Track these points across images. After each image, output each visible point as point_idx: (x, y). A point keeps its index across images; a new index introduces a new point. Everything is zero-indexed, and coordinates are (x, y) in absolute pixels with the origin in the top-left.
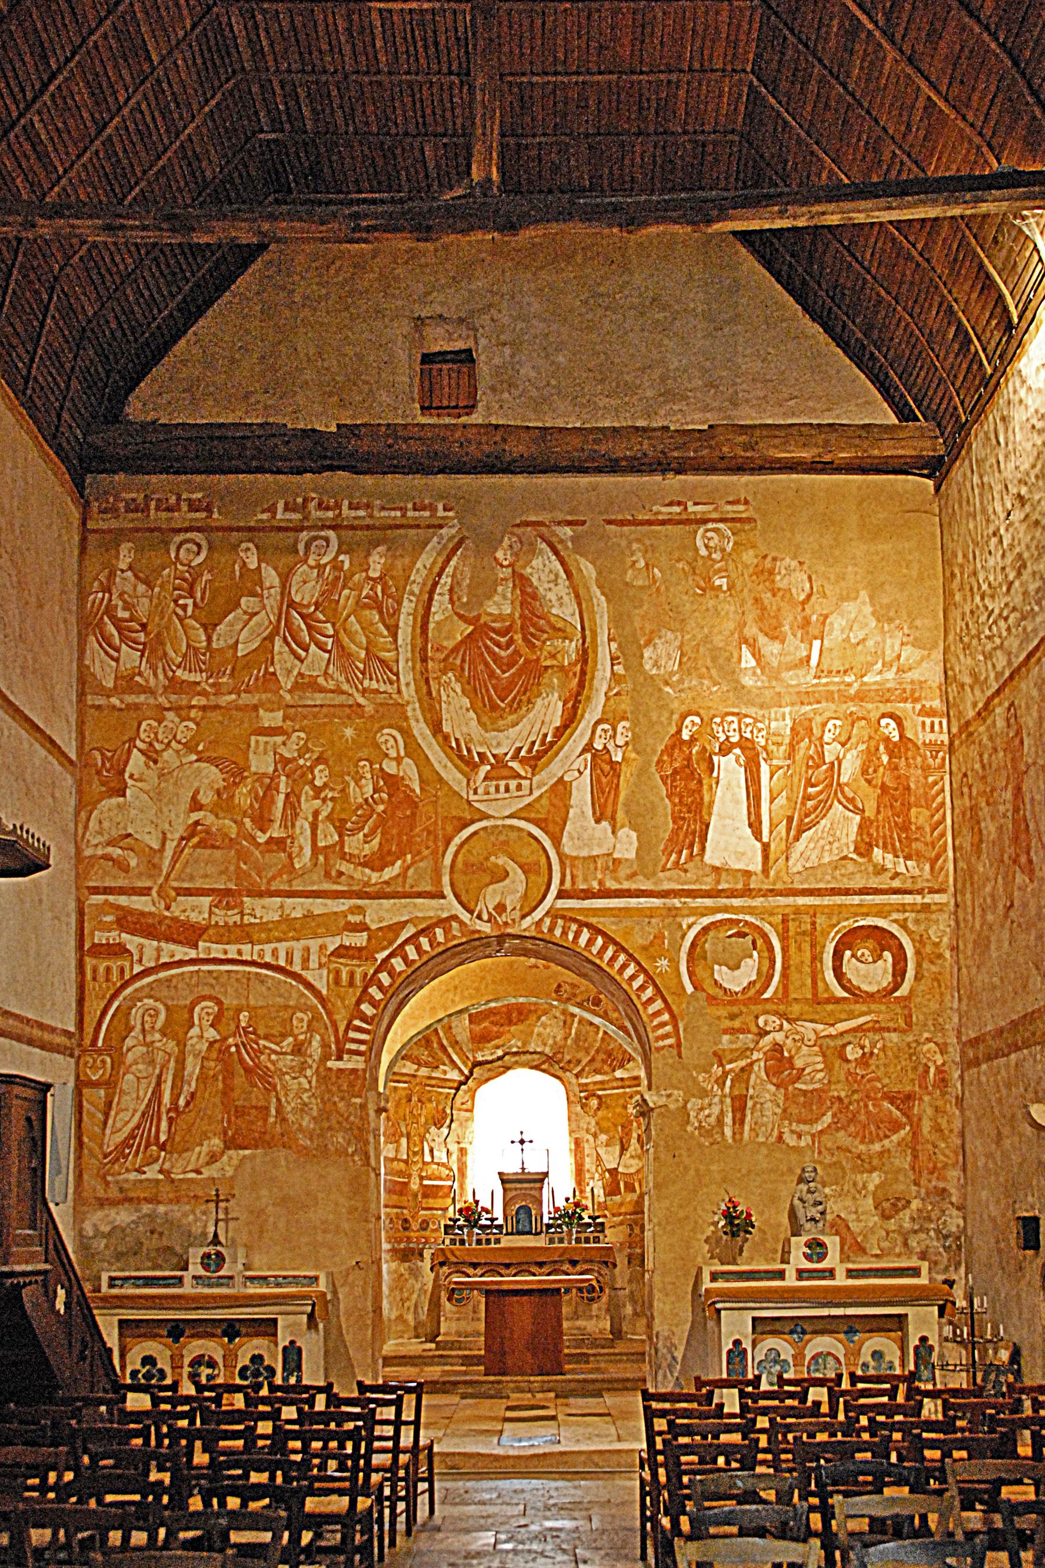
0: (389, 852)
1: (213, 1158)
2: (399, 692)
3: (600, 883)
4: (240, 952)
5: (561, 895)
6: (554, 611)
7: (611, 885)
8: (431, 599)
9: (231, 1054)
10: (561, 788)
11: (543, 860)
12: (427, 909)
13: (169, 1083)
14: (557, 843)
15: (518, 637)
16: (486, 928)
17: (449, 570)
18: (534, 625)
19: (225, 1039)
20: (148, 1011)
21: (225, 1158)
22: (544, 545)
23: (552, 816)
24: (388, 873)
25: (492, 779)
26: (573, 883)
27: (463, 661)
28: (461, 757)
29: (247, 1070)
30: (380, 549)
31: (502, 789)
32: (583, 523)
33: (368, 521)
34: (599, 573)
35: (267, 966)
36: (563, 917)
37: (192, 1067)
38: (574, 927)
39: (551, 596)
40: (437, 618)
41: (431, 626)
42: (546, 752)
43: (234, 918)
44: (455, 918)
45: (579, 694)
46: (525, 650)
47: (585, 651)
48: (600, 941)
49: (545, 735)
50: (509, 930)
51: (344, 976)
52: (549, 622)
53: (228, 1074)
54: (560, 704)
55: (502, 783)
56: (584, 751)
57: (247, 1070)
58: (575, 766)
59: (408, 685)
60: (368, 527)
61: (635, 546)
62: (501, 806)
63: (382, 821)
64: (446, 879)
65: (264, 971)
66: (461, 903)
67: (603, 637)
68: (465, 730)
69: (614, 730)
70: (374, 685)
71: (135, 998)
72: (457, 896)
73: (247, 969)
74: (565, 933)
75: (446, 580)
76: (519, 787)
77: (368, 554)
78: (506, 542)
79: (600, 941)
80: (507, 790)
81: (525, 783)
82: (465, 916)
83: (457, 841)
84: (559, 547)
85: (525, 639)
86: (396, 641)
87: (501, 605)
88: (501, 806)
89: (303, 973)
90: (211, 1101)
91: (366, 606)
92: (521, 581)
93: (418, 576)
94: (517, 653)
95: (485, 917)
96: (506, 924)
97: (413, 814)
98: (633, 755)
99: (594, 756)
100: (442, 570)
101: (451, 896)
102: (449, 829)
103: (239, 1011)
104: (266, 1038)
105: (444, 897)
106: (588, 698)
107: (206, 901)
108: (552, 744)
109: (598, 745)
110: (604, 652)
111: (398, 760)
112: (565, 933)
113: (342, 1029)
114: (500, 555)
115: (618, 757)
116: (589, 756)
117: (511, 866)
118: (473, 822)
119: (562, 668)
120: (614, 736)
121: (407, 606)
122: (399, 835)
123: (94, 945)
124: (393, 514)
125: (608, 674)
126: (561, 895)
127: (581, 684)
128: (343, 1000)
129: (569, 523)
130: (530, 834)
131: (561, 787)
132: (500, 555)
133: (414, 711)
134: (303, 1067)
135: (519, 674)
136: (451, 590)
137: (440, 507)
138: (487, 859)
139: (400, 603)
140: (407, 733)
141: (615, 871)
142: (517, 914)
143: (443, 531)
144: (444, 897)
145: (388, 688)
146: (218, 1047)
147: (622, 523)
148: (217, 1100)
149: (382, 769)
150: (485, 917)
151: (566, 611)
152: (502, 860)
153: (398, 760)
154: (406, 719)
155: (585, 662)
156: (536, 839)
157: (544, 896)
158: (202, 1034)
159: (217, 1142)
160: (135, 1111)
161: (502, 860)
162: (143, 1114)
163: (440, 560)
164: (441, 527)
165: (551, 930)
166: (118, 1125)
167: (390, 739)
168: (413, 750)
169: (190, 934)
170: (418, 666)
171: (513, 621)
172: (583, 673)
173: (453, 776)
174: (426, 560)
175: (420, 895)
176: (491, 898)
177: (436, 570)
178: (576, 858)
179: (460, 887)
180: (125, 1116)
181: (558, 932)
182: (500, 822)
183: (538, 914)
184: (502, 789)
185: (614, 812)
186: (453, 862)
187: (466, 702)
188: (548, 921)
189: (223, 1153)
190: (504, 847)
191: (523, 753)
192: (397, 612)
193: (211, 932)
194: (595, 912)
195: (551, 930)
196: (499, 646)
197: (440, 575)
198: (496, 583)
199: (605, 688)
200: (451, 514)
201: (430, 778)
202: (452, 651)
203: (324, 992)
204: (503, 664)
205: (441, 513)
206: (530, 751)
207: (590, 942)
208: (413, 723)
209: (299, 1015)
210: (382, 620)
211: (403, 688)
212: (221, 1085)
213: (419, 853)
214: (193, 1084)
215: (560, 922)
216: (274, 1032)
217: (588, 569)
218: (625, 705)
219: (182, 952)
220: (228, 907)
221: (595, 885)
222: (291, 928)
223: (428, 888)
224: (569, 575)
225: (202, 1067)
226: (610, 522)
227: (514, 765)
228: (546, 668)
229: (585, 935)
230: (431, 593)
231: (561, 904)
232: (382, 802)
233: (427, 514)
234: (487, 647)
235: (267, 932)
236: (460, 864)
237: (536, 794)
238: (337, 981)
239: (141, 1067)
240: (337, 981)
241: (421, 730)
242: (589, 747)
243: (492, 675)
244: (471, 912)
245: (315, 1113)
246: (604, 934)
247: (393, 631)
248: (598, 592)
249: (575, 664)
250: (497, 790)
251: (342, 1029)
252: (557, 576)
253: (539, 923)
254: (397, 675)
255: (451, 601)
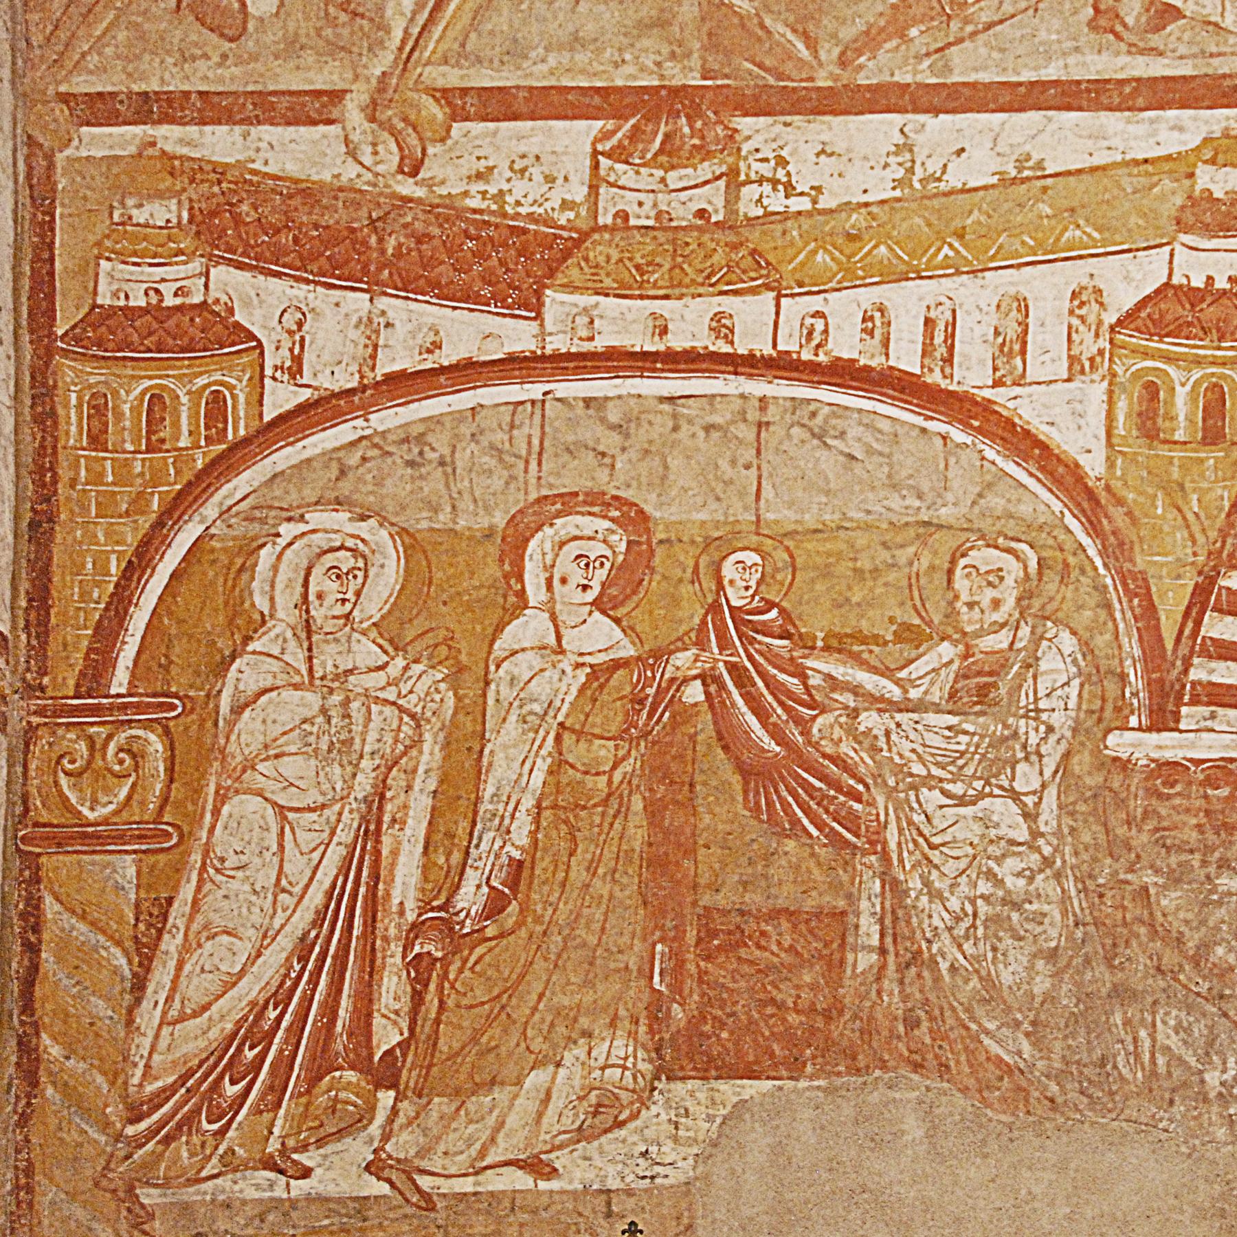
1: (604, 1114)
4: (721, 325)
9: (684, 715)
13: (417, 826)
19: (660, 654)
20: (322, 555)
21: (657, 1113)
29: (756, 773)
35: (844, 374)
37: (515, 767)
43: (692, 193)
51: (1183, 405)
53: (671, 783)
57: (756, 773)
65: (825, 394)
71: (265, 514)
73: (757, 387)
89: (1000, 396)
90: (600, 900)
103: (718, 546)
104: (837, 645)
107: (580, 134)
113: (1171, 607)
123: (98, 317)
128: (1176, 492)
134: (998, 761)
146: (629, 695)
148: (628, 892)
158: (555, 642)
159: (618, 1054)
160: (267, 936)
162: (303, 949)
166: (195, 989)
169: (508, 261)
180: (223, 955)
189: (644, 1097)
193: (598, 250)
203: (1094, 465)
209: (984, 557)
212: (637, 833)
214: (521, 832)
216: (875, 622)
219: (469, 332)
220: (670, 154)
222: (936, 230)
225: (559, 765)
235: (857, 246)
238: (1150, 422)
239: (290, 767)
240: (1150, 422)
245: (1053, 935)
251: (1171, 607)
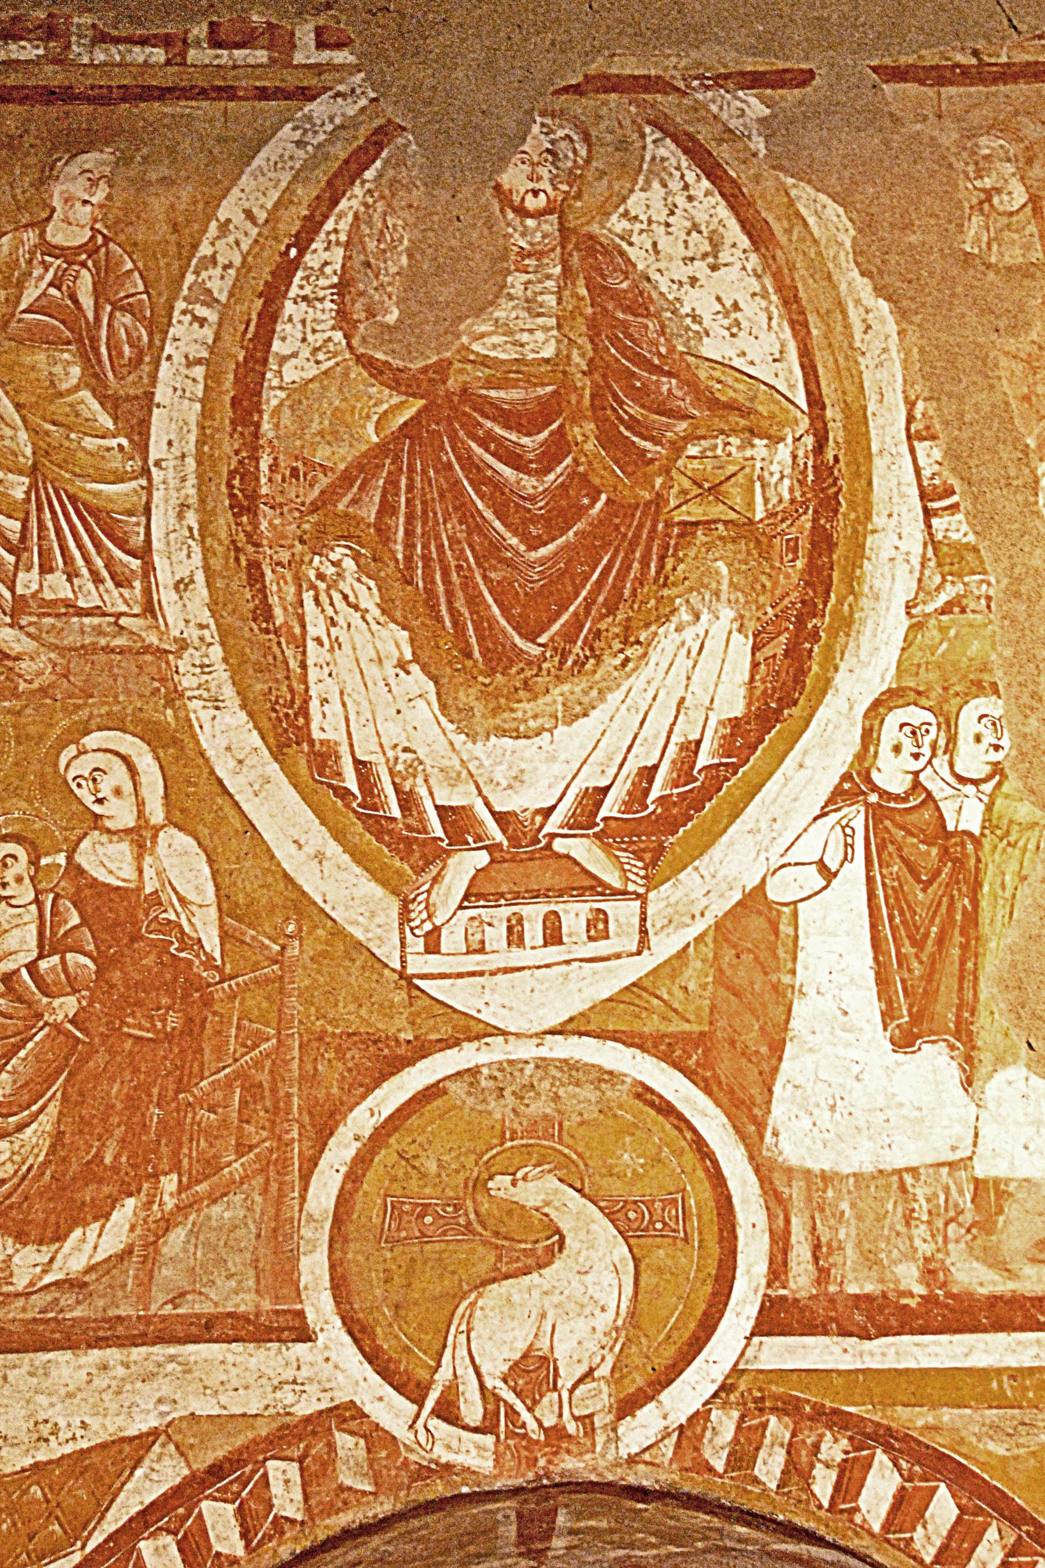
0: (93, 1171)
2: (150, 608)
3: (930, 1272)
5: (775, 1318)
6: (709, 349)
7: (972, 1276)
8: (269, 317)
10: (758, 930)
11: (698, 1194)
12: (240, 1383)
14: (749, 1117)
15: (584, 433)
16: (473, 1455)
17: (338, 224)
18: (640, 395)
22: (668, 150)
23: (727, 1022)
24: (84, 1249)
25: (495, 898)
26: (823, 1275)
27: (387, 508)
28: (378, 826)
30: (89, 160)
31: (534, 932)
32: (806, 78)
33: (52, 76)
34: (866, 226)
36: (789, 1407)
38: (834, 1448)
39: (699, 301)
40: (291, 374)
41: (273, 398)
42: (696, 802)
44: (347, 1415)
45: (809, 609)
46: (609, 471)
47: (824, 472)
48: (944, 1508)
49: (692, 748)
50: (570, 1464)
52: (692, 385)
54: (742, 645)
55: (534, 913)
56: (838, 797)
58: (808, 850)
59: (182, 586)
60: (50, 95)
61: (987, 144)
62: (528, 994)
63: (68, 1055)
64: (314, 1266)
66: (372, 1357)
67: (887, 427)
68: (393, 732)
69: (949, 725)
70: (58, 587)
72: (358, 1330)
74: (797, 1472)
75: (325, 256)
76: (598, 926)
77: (46, 177)
78: (536, 140)
79: (944, 1508)
80: (553, 936)
81: (622, 913)
82: (390, 1410)
83: (362, 1120)
84: (723, 153)
85: (609, 439)
86: (144, 449)
87: (522, 331)
88: (528, 994)
91: (37, 337)
92: (591, 259)
93: (226, 246)
94: (582, 481)
95: (473, 1411)
96: (556, 1434)
97: (192, 1027)
98: (1025, 811)
99: (877, 815)
100: (311, 227)
101: (333, 1334)
102: (332, 1075)
105: (305, 1335)
106: (846, 623)
108: (716, 776)
109: (891, 775)
110: (894, 478)
111: (141, 837)
112: (797, 1472)
114: (514, 178)
115: (966, 814)
116: (857, 817)
117: (573, 1212)
118: (421, 1050)
119: (744, 528)
120: (951, 747)
121: (186, 337)
122: (132, 1103)
124: (139, 54)
125: (914, 543)
126: (775, 1318)
127: (818, 579)
129: (754, 81)
130: (644, 1093)
131: (757, 924)
132: (514, 178)
133: (204, 672)
135: (590, 548)
136: (343, 287)
137: (305, 34)
138: (479, 1185)
139: (159, 326)
140: (175, 745)
141: (985, 1225)
142: (597, 1399)
143: (317, 108)
144: (305, 1335)
145: (114, 599)
147: (940, 76)
149: (75, 870)
150: (473, 1411)
151: (757, 349)
152: (537, 1190)
153: (141, 837)
154: (175, 697)
155: (828, 505)
156: (666, 1109)
157: (708, 1326)
161: (537, 1190)
163: (306, 194)
164: (307, 95)
165: (741, 1458)
167: (111, 771)
168: (197, 800)
170: (223, 522)
171: (565, 383)
172: (822, 541)
173: (347, 892)
174: (251, 197)
175: (206, 1329)
176: (494, 1333)
177: (291, 223)
178: (827, 1178)
179: (372, 1295)
181: (770, 1467)
182: (526, 1051)
183: (686, 1395)
184: (534, 932)
185: (967, 1008)
186: (344, 1199)
187: (396, 640)
188: (725, 1424)
190: (545, 1144)
191: (610, 808)
192: (148, 356)
194: (920, 1385)
195: (741, 1458)
196: (515, 460)
197: (303, 241)
198: (502, 263)
199: (904, 588)
200: (341, 57)
201: (260, 897)
202: (346, 479)
204: (539, 519)
205: (306, 52)
206: (638, 796)
207: (907, 1508)
208: (198, 710)
210: (94, 380)
211: (167, 597)
213: (212, 1167)
215: (777, 1427)
217: (828, 219)
218: (983, 644)
221: (909, 1278)
223: (244, 1303)
224: (758, 235)
226: (898, 74)
227: (581, 849)
228: (689, 528)
229: (881, 1485)
230: (273, 297)
231: (781, 1353)
232: (73, 987)
233: (261, 56)
234: (469, 463)
236: (370, 1206)
237: (665, 946)
241: (228, 735)
242: (854, 786)
243: (491, 552)
244: (413, 1390)
246: (960, 1478)
247: (135, 416)
248: (864, 287)
249: (792, 513)
250: (515, 936)
252: (716, 243)
253: (691, 1431)
254: (145, 553)
255: (344, 319)
